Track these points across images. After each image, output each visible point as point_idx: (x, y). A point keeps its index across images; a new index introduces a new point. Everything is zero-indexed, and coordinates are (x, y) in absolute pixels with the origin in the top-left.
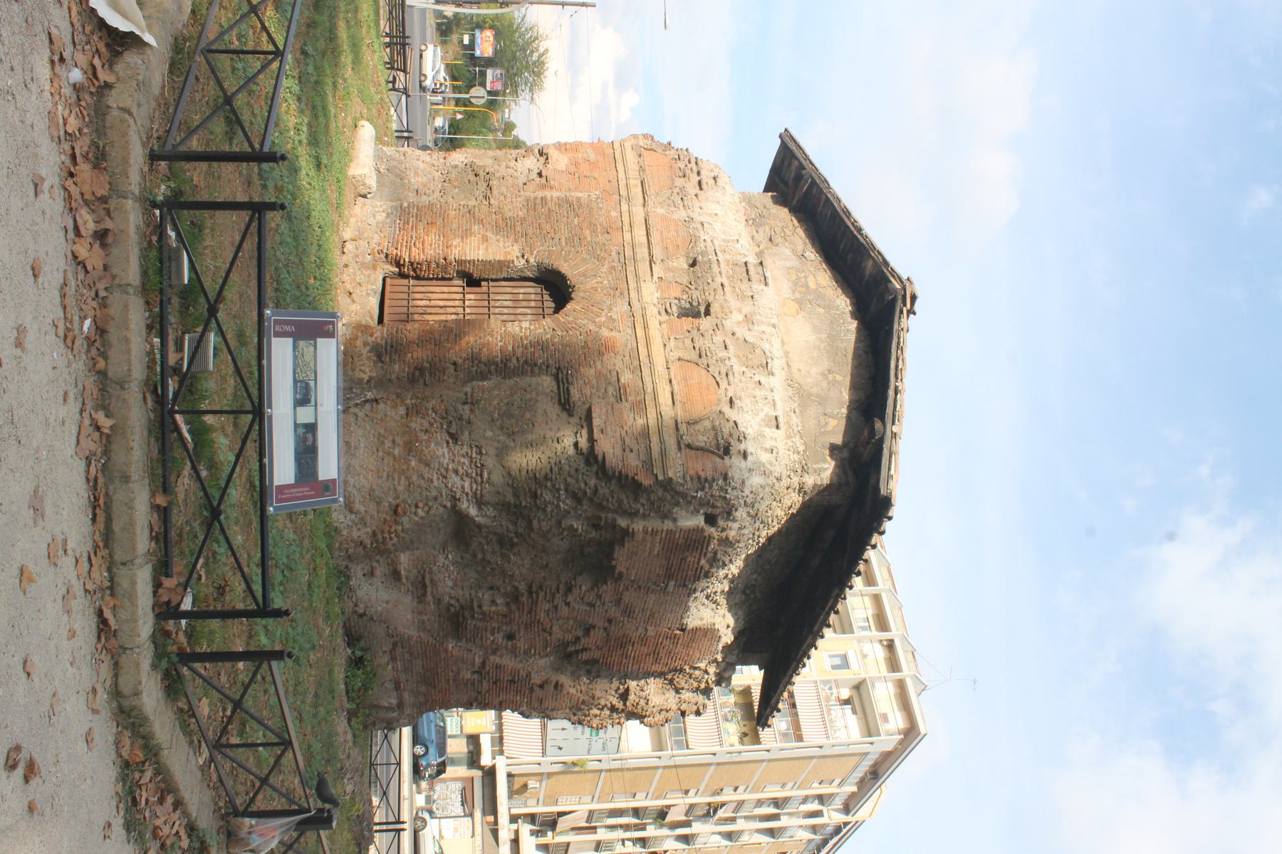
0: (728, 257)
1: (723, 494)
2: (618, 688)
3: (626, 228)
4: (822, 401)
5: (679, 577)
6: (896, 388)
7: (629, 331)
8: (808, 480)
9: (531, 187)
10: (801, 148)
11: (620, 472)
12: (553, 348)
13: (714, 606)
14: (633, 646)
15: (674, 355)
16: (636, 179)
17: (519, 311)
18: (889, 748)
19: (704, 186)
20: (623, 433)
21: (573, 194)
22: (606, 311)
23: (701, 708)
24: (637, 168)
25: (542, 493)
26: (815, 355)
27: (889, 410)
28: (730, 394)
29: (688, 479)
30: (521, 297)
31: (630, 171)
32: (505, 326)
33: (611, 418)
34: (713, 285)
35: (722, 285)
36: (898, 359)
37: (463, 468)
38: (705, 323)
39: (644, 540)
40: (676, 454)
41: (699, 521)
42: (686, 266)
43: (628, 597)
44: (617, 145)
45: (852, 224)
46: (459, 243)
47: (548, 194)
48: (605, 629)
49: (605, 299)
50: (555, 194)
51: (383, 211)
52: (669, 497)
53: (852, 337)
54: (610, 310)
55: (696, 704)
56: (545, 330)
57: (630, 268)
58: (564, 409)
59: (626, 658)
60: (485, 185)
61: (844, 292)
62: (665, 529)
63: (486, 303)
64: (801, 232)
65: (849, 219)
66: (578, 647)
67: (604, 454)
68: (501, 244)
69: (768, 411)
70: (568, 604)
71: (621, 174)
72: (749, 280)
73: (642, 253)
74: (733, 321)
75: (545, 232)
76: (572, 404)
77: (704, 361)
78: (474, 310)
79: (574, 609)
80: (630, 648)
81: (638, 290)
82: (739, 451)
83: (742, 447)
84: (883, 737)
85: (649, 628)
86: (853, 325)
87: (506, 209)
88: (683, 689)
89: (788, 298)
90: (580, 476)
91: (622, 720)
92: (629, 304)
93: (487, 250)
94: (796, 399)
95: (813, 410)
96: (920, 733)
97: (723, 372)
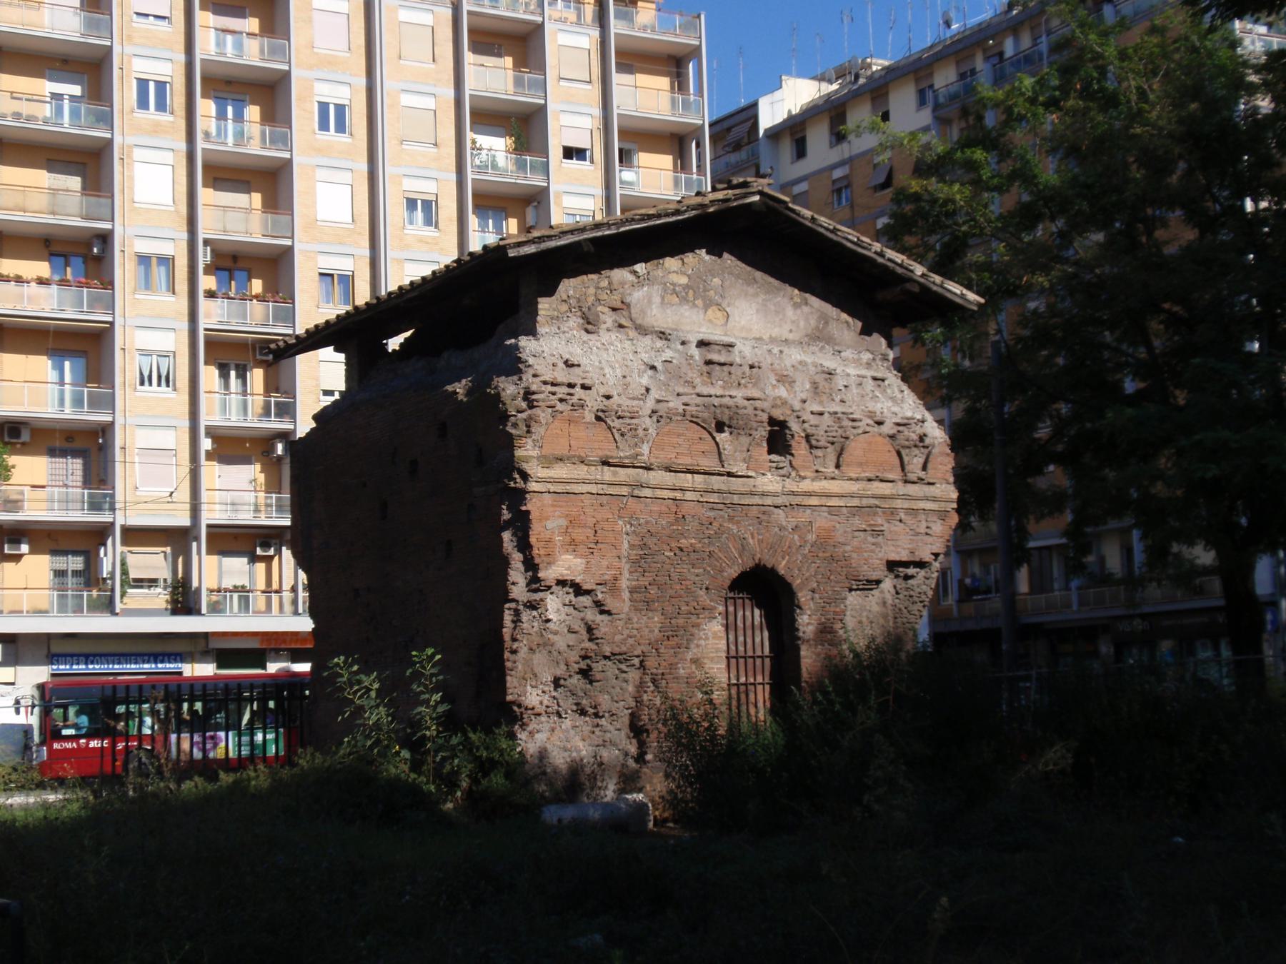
3: (679, 495)
4: (825, 319)
6: (876, 253)
7: (808, 511)
9: (610, 604)
12: (830, 593)
15: (831, 470)
16: (602, 472)
17: (740, 624)
19: (587, 382)
21: (626, 554)
26: (772, 308)
33: (899, 543)
34: (750, 411)
38: (794, 426)
40: (938, 488)
45: (667, 215)
47: (624, 583)
49: (773, 533)
50: (626, 575)
57: (736, 499)
60: (604, 662)
63: (742, 661)
68: (702, 642)
69: (870, 384)
71: (593, 489)
72: (731, 365)
73: (717, 483)
75: (682, 592)
78: (750, 673)
81: (764, 494)
87: (651, 635)
92: (776, 507)
94: (821, 344)
97: (851, 424)
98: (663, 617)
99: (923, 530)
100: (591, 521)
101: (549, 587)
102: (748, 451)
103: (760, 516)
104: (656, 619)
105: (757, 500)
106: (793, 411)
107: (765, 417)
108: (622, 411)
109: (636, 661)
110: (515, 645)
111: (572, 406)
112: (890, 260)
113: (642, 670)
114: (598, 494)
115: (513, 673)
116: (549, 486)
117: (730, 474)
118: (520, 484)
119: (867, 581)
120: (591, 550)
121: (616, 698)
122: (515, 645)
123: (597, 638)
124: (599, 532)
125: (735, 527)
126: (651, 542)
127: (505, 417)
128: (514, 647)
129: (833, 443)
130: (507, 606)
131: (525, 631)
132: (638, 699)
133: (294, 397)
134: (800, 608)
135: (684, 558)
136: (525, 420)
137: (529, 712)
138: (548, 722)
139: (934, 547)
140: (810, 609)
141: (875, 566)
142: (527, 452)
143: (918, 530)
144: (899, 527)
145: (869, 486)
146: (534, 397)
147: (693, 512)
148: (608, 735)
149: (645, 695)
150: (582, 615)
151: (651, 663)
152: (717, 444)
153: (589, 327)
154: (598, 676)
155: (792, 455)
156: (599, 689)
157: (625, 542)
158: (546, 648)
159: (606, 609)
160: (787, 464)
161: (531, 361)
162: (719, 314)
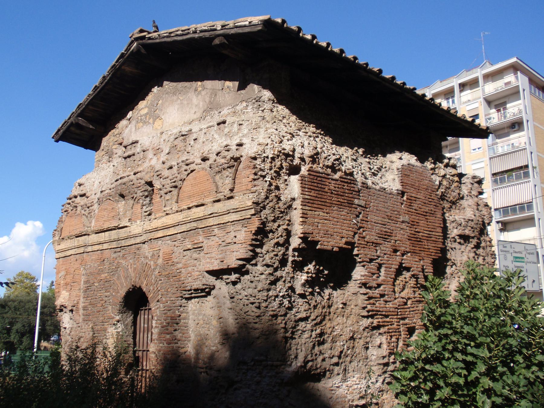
0: (121, 172)
1: (269, 160)
2: (460, 243)
4: (214, 93)
5: (351, 195)
8: (266, 96)
11: (251, 245)
13: (383, 170)
14: (419, 232)
18: (526, 79)
20: (224, 244)
21: (82, 287)
22: (147, 261)
23: (476, 180)
24: (69, 240)
25: (272, 311)
27: (207, 34)
28: (199, 161)
29: (255, 188)
30: (146, 326)
31: (71, 246)
32: (154, 340)
33: (213, 255)
36: (177, 35)
37: (255, 377)
39: (313, 224)
41: (294, 179)
42: (124, 202)
43: (371, 236)
44: (58, 256)
47: (81, 305)
48: (403, 255)
50: (82, 300)
52: (271, 204)
54: (146, 258)
55: (472, 184)
56: (157, 308)
57: (123, 243)
58: (209, 294)
59: (431, 237)
62: (301, 207)
66: (421, 275)
67: (237, 259)
70: (379, 286)
72: (134, 155)
73: (114, 234)
74: (155, 162)
76: (204, 287)
77: (179, 183)
79: (384, 281)
80: (421, 234)
82: (237, 150)
83: (234, 147)
84: (520, 84)
85: (401, 220)
88: (459, 194)
89: (153, 127)
90: (256, 279)
91: (488, 239)
92: (144, 243)
96: (516, 61)
97: (186, 167)
103: (135, 252)
105: (132, 241)
107: (143, 182)
112: (202, 31)
125: (124, 262)
135: (102, 287)
139: (238, 253)
141: (196, 277)
143: (227, 241)
145: (189, 213)
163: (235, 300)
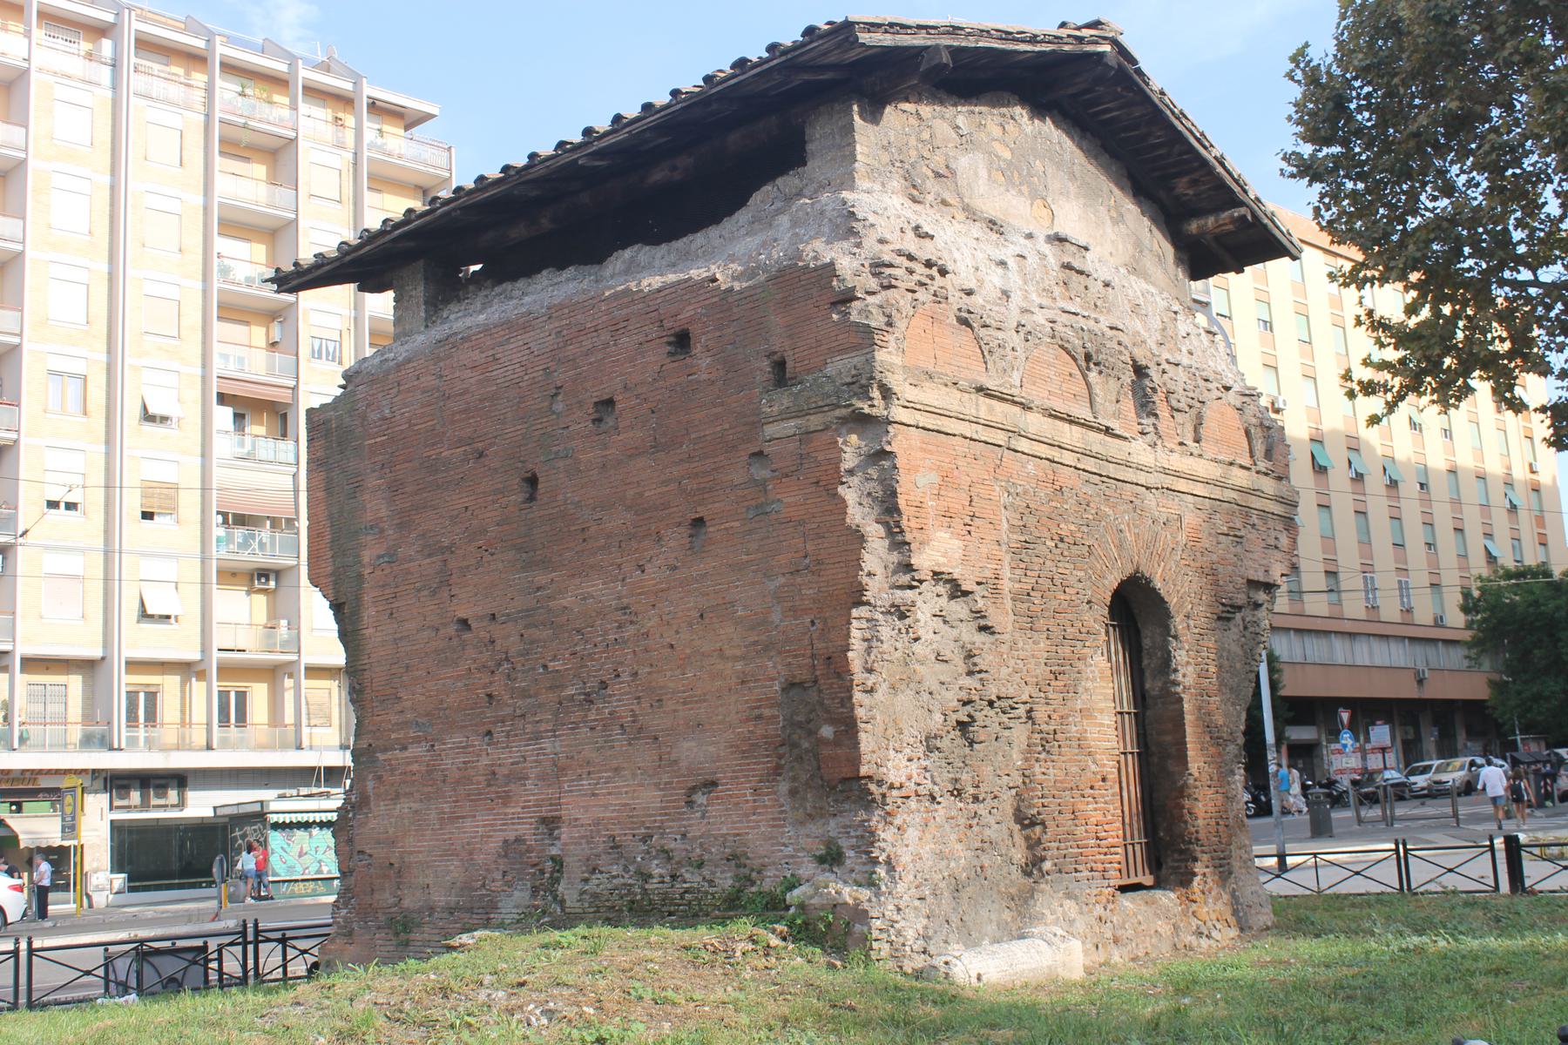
4: (1138, 244)
6: (1215, 158)
10: (891, 25)
31: (961, 409)
33: (1255, 556)
35: (1111, 328)
45: (1023, 41)
46: (1094, 762)
47: (1006, 585)
50: (1006, 573)
51: (1061, 906)
53: (1068, 143)
57: (1111, 470)
61: (1007, 106)
64: (926, 110)
65: (1017, 40)
68: (1089, 684)
73: (1096, 441)
86: (1048, 128)
92: (1147, 488)
93: (1102, 711)
95: (1149, 263)
98: (1048, 642)
99: (1272, 542)
100: (965, 481)
101: (921, 582)
102: (1118, 402)
104: (1042, 645)
105: (1129, 475)
106: (1154, 355)
108: (989, 316)
109: (1021, 711)
110: (871, 680)
111: (935, 295)
113: (1029, 724)
114: (971, 439)
115: (869, 726)
116: (918, 415)
117: (1108, 431)
118: (879, 409)
119: (1232, 606)
120: (968, 528)
121: (998, 772)
122: (871, 680)
123: (980, 672)
124: (975, 499)
126: (1031, 520)
127: (848, 297)
128: (870, 683)
129: (1191, 407)
130: (855, 612)
131: (885, 657)
132: (1027, 773)
133: (16, 508)
134: (1175, 637)
136: (881, 307)
137: (895, 793)
138: (919, 811)
140: (1187, 641)
142: (889, 358)
144: (1253, 535)
146: (888, 271)
147: (1070, 483)
148: (987, 832)
149: (1037, 765)
150: (955, 632)
151: (1040, 714)
152: (1088, 385)
153: (915, 193)
154: (981, 735)
155: (1156, 415)
156: (981, 755)
157: (1004, 520)
158: (911, 685)
159: (990, 624)
160: (1151, 429)
161: (872, 219)
162: (1045, 212)
163: (1247, 634)
